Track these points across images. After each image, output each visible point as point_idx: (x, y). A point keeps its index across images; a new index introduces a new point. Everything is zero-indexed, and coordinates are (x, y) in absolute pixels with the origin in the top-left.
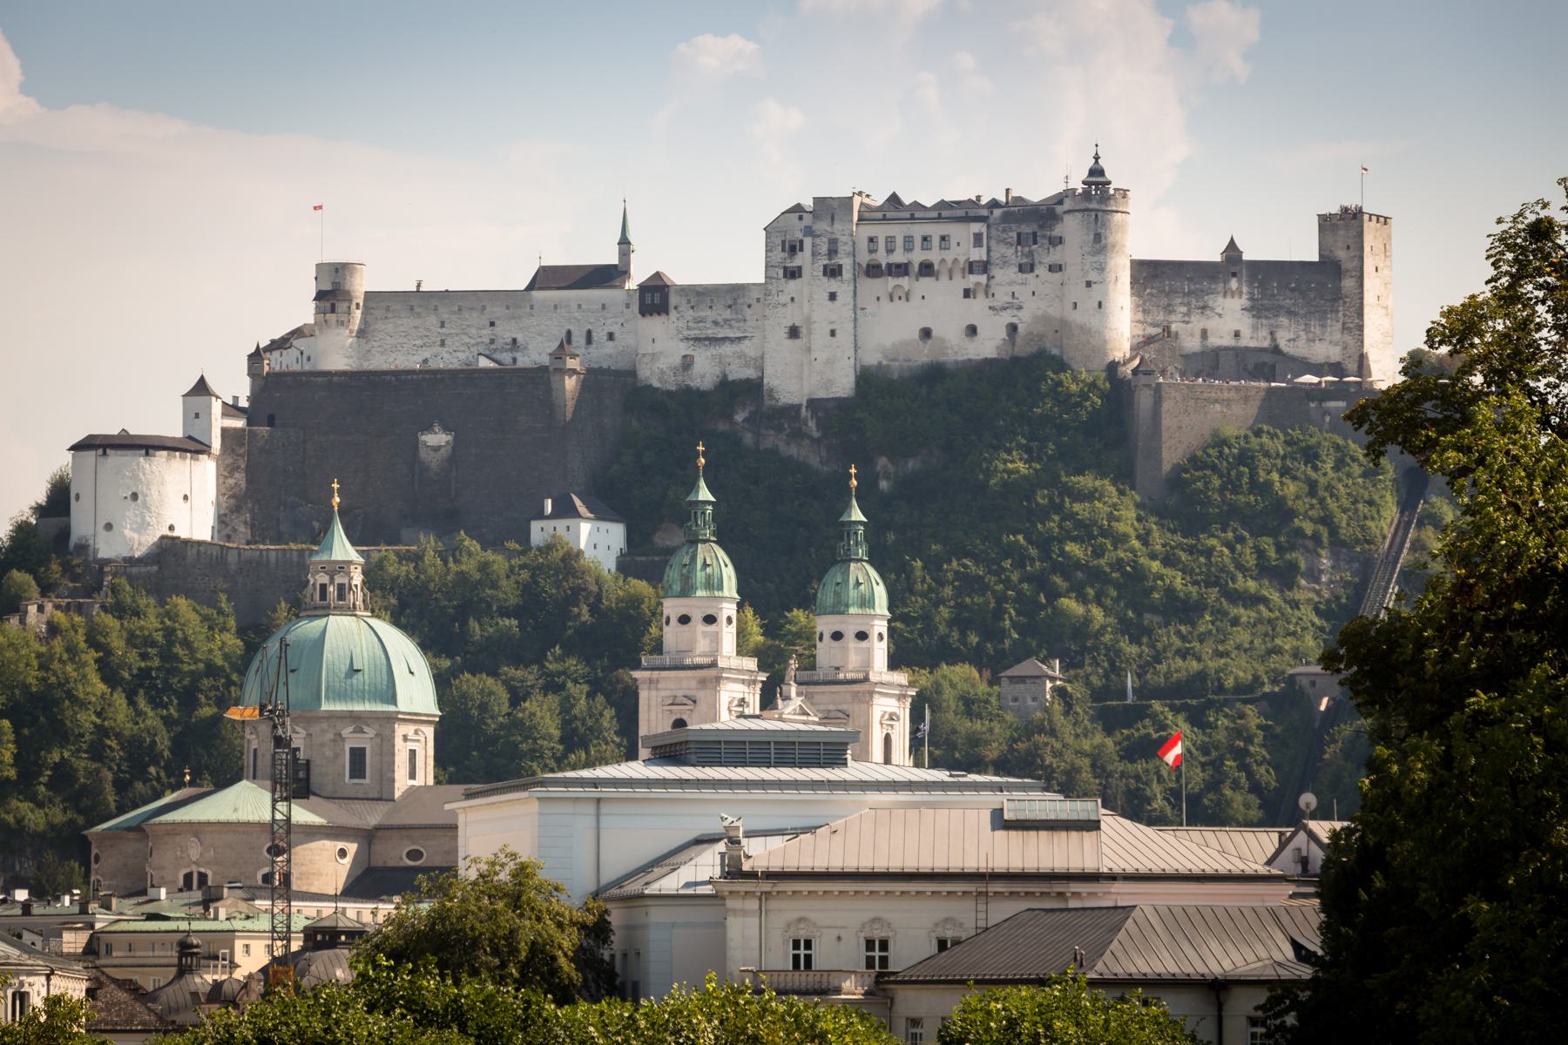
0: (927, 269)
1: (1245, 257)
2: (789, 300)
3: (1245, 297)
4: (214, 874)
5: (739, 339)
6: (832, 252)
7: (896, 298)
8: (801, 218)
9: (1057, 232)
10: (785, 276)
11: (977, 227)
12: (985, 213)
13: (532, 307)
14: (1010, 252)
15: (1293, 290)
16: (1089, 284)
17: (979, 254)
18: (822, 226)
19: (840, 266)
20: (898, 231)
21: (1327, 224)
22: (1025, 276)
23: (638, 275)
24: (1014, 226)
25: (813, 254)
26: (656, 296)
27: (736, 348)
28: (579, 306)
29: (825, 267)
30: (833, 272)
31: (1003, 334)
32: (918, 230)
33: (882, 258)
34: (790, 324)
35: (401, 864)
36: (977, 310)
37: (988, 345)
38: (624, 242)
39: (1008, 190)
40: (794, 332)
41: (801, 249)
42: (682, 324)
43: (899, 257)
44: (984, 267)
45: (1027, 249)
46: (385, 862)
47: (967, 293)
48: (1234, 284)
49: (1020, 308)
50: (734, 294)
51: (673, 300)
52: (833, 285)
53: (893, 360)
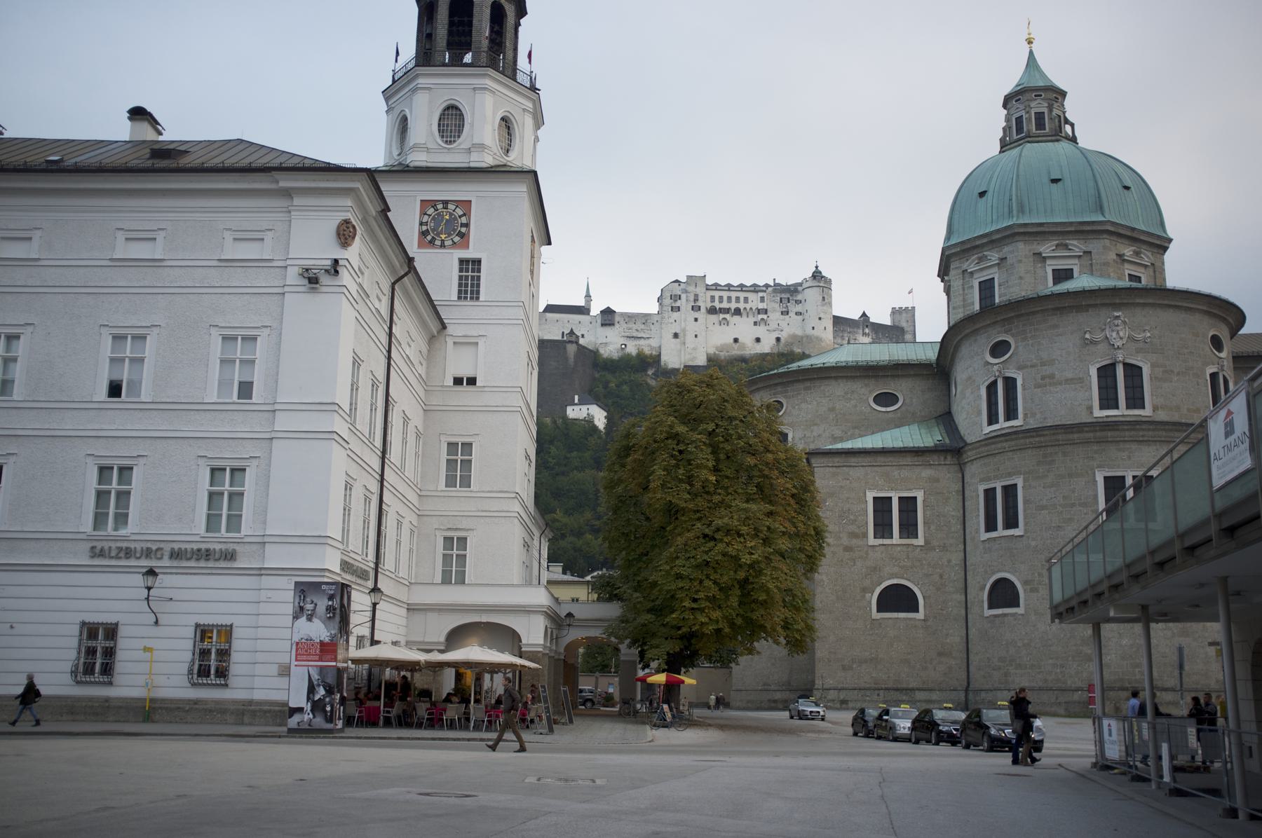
0: (738, 312)
1: (871, 320)
2: (673, 321)
3: (870, 337)
4: (1153, 366)
5: (648, 338)
6: (696, 300)
7: (722, 324)
8: (679, 285)
9: (799, 297)
10: (672, 310)
11: (761, 294)
12: (764, 289)
13: (546, 320)
14: (777, 306)
15: (887, 337)
16: (820, 319)
17: (761, 306)
18: (691, 288)
19: (700, 307)
20: (725, 294)
21: (895, 312)
22: (784, 317)
23: (595, 310)
24: (778, 294)
25: (687, 300)
26: (608, 315)
27: (647, 342)
28: (568, 322)
29: (693, 306)
30: (696, 308)
31: (774, 341)
32: (734, 295)
33: (717, 305)
34: (674, 332)
36: (760, 331)
37: (767, 346)
38: (588, 296)
39: (774, 280)
40: (676, 336)
41: (680, 299)
42: (621, 329)
43: (725, 305)
44: (766, 311)
45: (784, 305)
47: (755, 323)
48: (867, 331)
49: (782, 331)
50: (645, 318)
51: (617, 318)
52: (696, 315)
53: (721, 352)
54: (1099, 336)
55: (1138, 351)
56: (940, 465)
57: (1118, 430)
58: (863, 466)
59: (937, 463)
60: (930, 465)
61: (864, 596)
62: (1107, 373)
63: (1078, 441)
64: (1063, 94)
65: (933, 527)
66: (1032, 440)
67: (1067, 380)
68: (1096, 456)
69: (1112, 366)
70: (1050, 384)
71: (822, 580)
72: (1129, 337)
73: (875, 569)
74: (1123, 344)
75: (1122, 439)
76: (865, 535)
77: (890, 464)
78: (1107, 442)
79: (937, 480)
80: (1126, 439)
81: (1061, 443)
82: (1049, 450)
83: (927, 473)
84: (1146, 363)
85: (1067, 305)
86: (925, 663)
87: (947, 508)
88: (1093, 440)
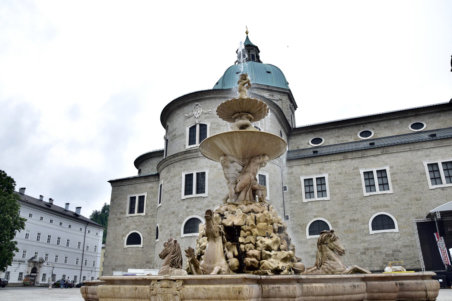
4: (212, 124)
35: (309, 147)
46: (298, 147)
54: (191, 114)
55: (206, 118)
56: (154, 181)
57: (191, 153)
58: (127, 185)
59: (153, 181)
60: (151, 182)
61: (123, 238)
62: (193, 129)
63: (177, 160)
64: (256, 47)
65: (149, 208)
66: (165, 163)
67: (179, 135)
68: (183, 166)
69: (194, 127)
70: (175, 138)
71: (109, 233)
72: (202, 113)
73: (127, 227)
74: (199, 116)
75: (193, 157)
76: (125, 213)
77: (137, 183)
78: (187, 159)
79: (152, 188)
80: (194, 156)
81: (172, 162)
82: (170, 166)
83: (149, 185)
84: (209, 123)
85: (180, 104)
86: (141, 266)
87: (155, 199)
88: (182, 159)
